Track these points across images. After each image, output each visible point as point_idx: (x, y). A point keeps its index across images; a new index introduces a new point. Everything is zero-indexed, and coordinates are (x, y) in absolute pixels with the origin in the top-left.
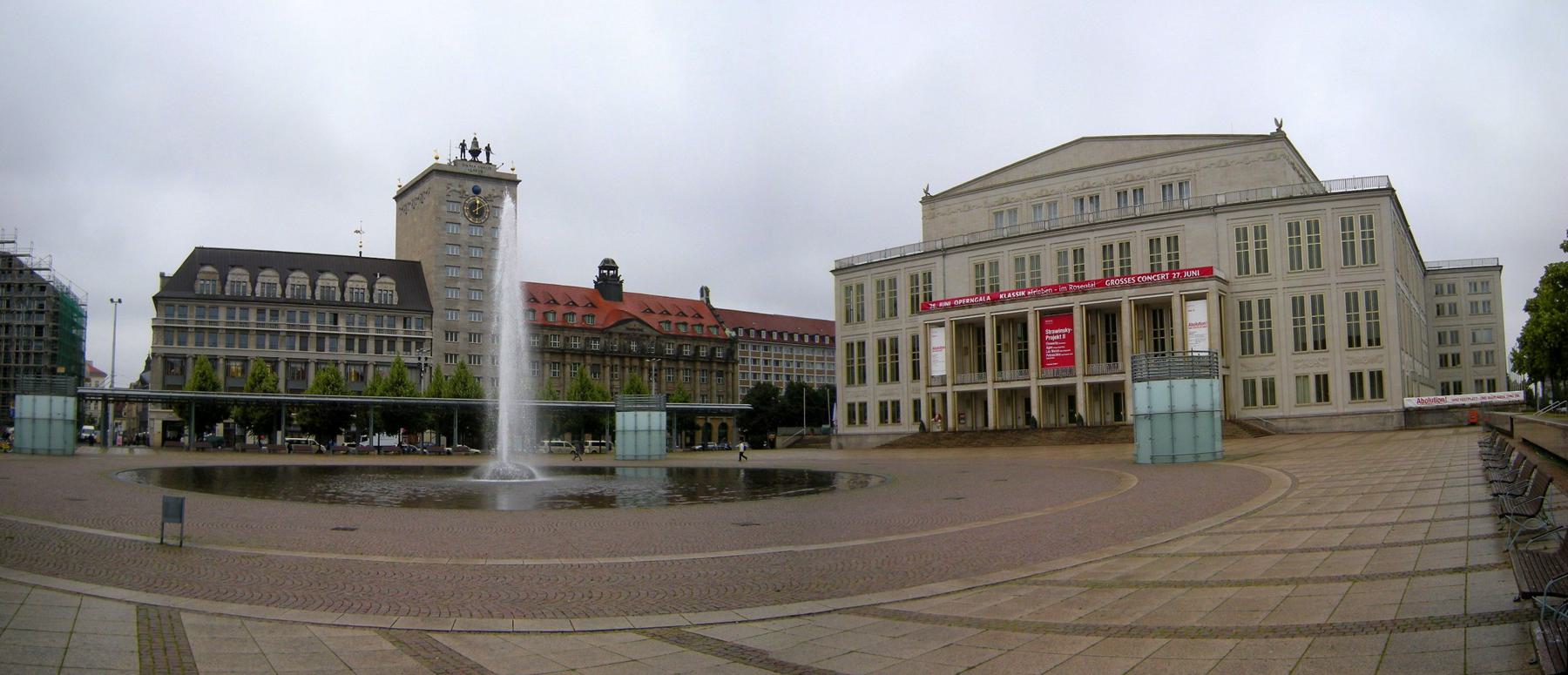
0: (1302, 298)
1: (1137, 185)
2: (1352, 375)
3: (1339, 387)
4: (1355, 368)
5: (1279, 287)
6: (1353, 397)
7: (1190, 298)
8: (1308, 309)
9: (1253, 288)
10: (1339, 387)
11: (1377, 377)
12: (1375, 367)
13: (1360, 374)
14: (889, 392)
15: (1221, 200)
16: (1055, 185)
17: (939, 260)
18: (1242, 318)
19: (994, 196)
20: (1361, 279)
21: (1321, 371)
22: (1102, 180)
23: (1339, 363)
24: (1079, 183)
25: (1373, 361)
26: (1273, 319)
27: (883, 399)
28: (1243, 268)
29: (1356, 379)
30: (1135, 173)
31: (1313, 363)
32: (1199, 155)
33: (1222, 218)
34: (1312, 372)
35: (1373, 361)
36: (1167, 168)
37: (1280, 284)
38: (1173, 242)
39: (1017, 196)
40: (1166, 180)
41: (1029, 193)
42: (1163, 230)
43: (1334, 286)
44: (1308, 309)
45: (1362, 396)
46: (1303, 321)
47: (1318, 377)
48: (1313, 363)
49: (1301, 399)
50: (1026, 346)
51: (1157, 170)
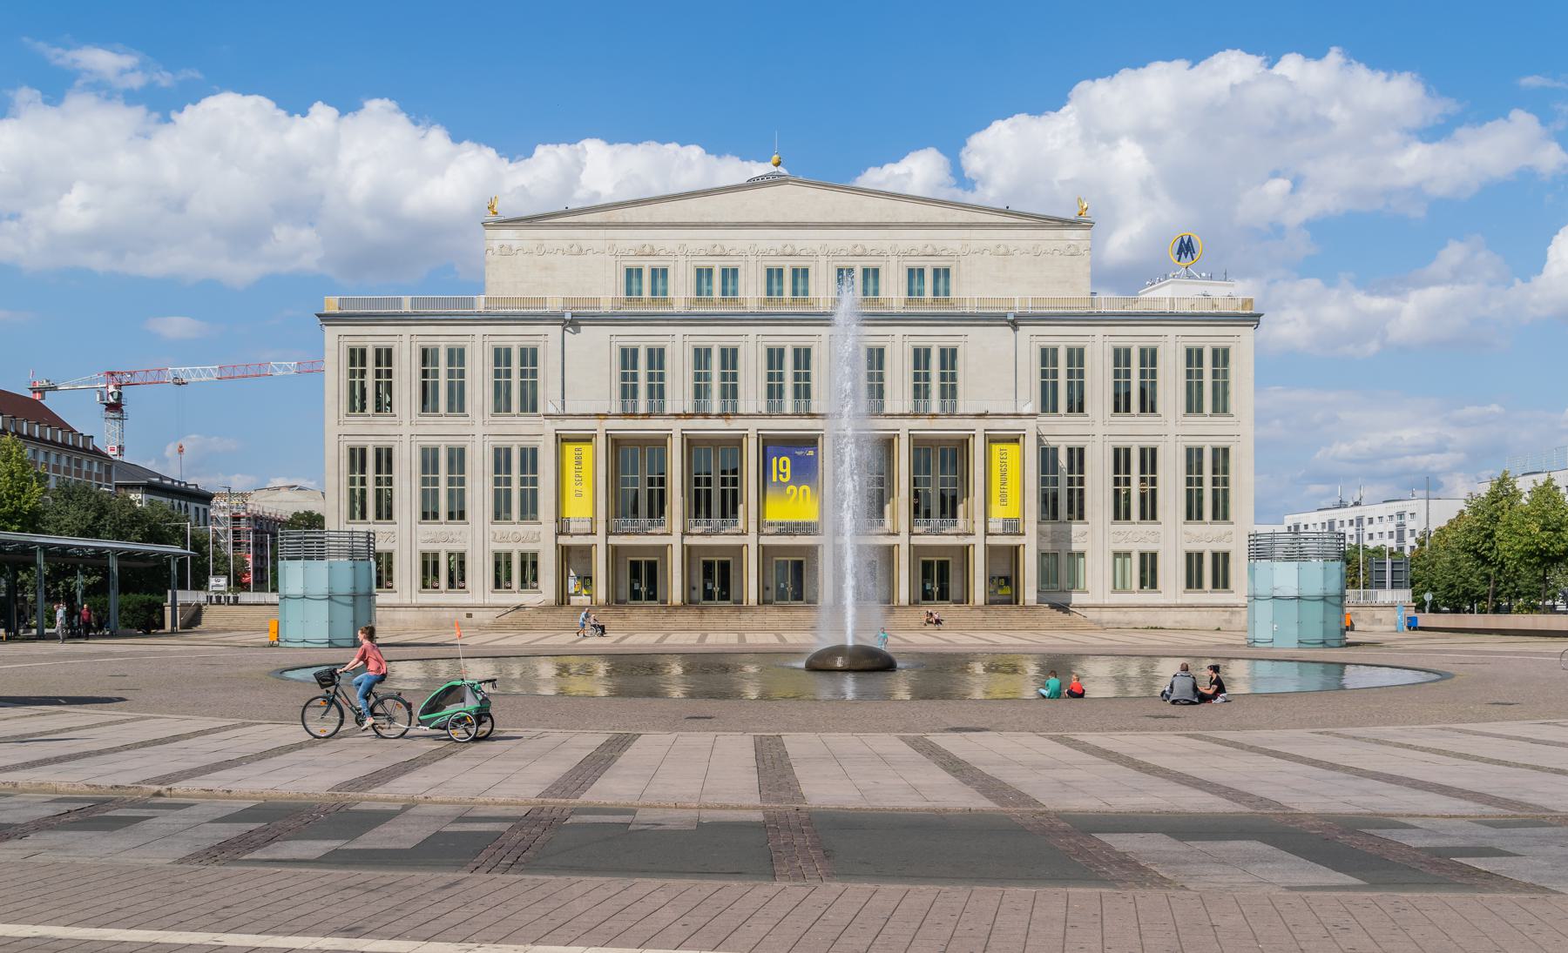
0: (1128, 451)
1: (871, 263)
2: (1189, 555)
3: (1171, 571)
4: (1195, 547)
5: (1099, 431)
6: (1189, 585)
7: (991, 440)
9: (1063, 430)
10: (1171, 571)
11: (1221, 561)
12: (1220, 547)
13: (1200, 555)
14: (443, 537)
16: (738, 241)
17: (555, 331)
19: (629, 240)
20: (1207, 431)
21: (1149, 547)
22: (816, 246)
24: (779, 246)
25: (1219, 540)
27: (430, 548)
28: (1048, 403)
29: (1193, 561)
30: (869, 246)
31: (1137, 536)
32: (966, 233)
33: (1024, 331)
34: (1136, 549)
35: (1219, 540)
36: (919, 245)
37: (1099, 430)
38: (949, 357)
39: (670, 246)
40: (916, 263)
41: (692, 246)
42: (935, 338)
43: (1171, 438)
45: (1200, 586)
46: (1200, 481)
47: (1143, 555)
49: (1120, 585)
51: (904, 246)
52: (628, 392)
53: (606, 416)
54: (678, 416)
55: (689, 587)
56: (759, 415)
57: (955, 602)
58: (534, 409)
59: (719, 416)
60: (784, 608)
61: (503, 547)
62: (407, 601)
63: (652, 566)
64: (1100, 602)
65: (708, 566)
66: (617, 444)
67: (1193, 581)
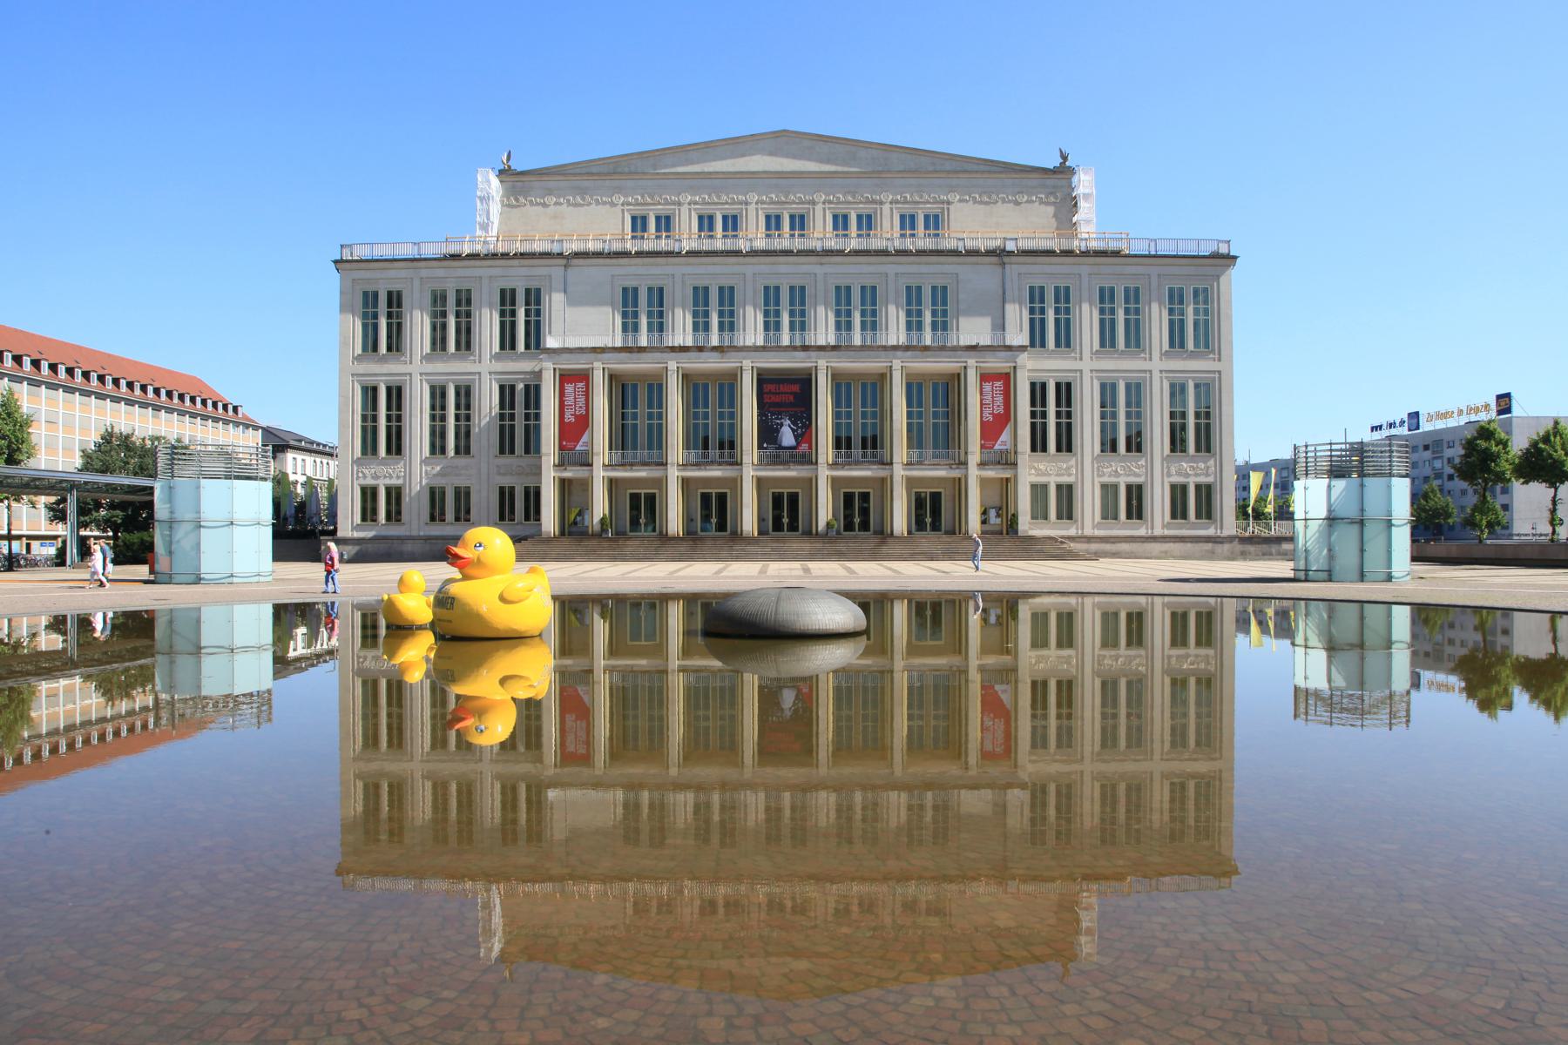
8: (1123, 399)
10: (1158, 502)
15: (1010, 246)
18: (1033, 404)
23: (1159, 471)
26: (1076, 408)
28: (1037, 338)
31: (1124, 471)
33: (1014, 269)
44: (1123, 399)
45: (1184, 516)
48: (1124, 471)
50: (837, 415)
52: (630, 327)
53: (603, 350)
54: (673, 349)
55: (688, 519)
56: (756, 349)
57: (947, 533)
58: (538, 346)
59: (714, 349)
60: (777, 540)
61: (507, 481)
62: (414, 533)
63: (651, 499)
64: (1088, 531)
65: (706, 498)
66: (613, 378)
67: (1178, 510)
